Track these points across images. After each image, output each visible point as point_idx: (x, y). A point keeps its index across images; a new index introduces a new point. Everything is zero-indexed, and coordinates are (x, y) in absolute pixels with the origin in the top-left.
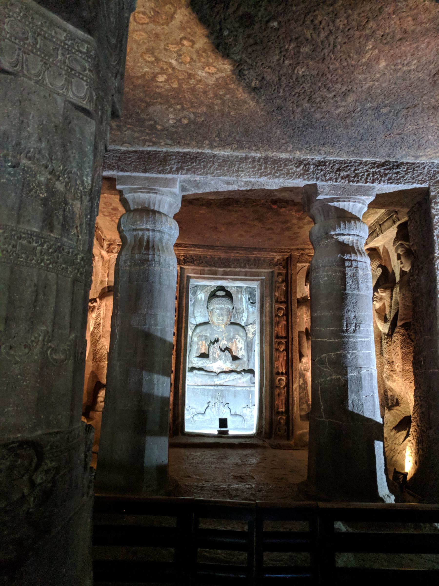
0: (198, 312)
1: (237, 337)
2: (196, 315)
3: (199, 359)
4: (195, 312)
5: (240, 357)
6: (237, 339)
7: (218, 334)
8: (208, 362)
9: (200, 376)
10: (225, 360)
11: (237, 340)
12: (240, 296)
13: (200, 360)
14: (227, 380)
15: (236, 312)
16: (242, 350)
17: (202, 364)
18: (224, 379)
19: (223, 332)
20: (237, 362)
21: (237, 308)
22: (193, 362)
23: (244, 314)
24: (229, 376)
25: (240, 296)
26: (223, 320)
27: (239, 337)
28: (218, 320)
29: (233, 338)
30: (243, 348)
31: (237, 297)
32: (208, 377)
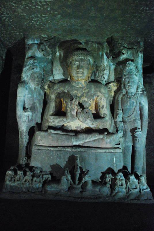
0: (56, 70)
1: (99, 94)
2: (54, 72)
3: (55, 117)
4: (54, 69)
5: (102, 116)
6: (98, 96)
7: (77, 90)
8: (65, 120)
9: (56, 136)
10: (85, 118)
11: (99, 98)
12: (101, 53)
13: (57, 119)
14: (87, 140)
15: (97, 70)
16: (104, 108)
17: (58, 122)
18: (84, 139)
19: (83, 88)
20: (99, 120)
21: (98, 65)
22: (50, 120)
23: (105, 72)
24: (90, 136)
25: (101, 53)
26: (83, 73)
27: (100, 94)
28: (78, 73)
29: (94, 95)
30: (105, 106)
31: (98, 54)
32: (64, 137)
